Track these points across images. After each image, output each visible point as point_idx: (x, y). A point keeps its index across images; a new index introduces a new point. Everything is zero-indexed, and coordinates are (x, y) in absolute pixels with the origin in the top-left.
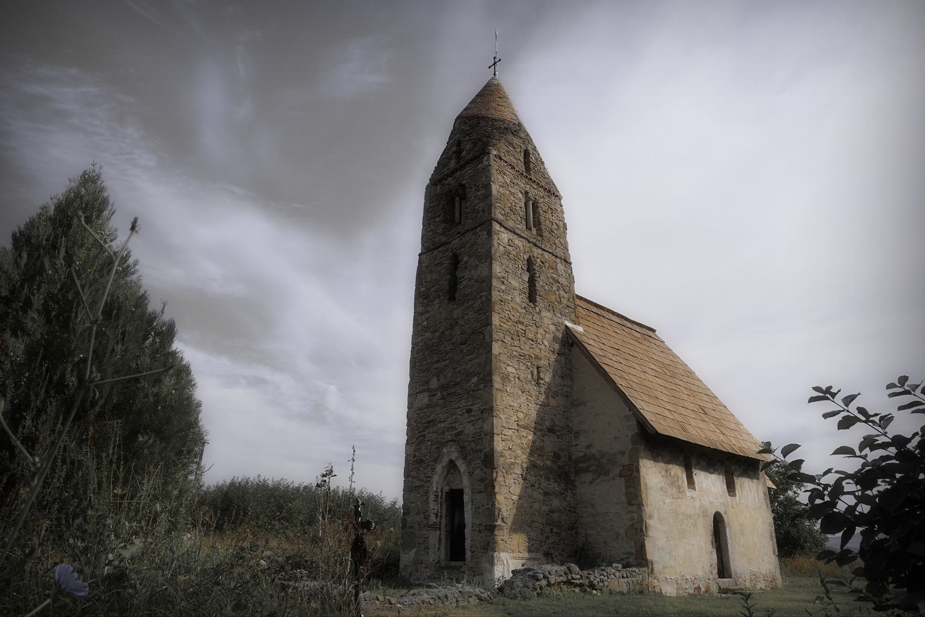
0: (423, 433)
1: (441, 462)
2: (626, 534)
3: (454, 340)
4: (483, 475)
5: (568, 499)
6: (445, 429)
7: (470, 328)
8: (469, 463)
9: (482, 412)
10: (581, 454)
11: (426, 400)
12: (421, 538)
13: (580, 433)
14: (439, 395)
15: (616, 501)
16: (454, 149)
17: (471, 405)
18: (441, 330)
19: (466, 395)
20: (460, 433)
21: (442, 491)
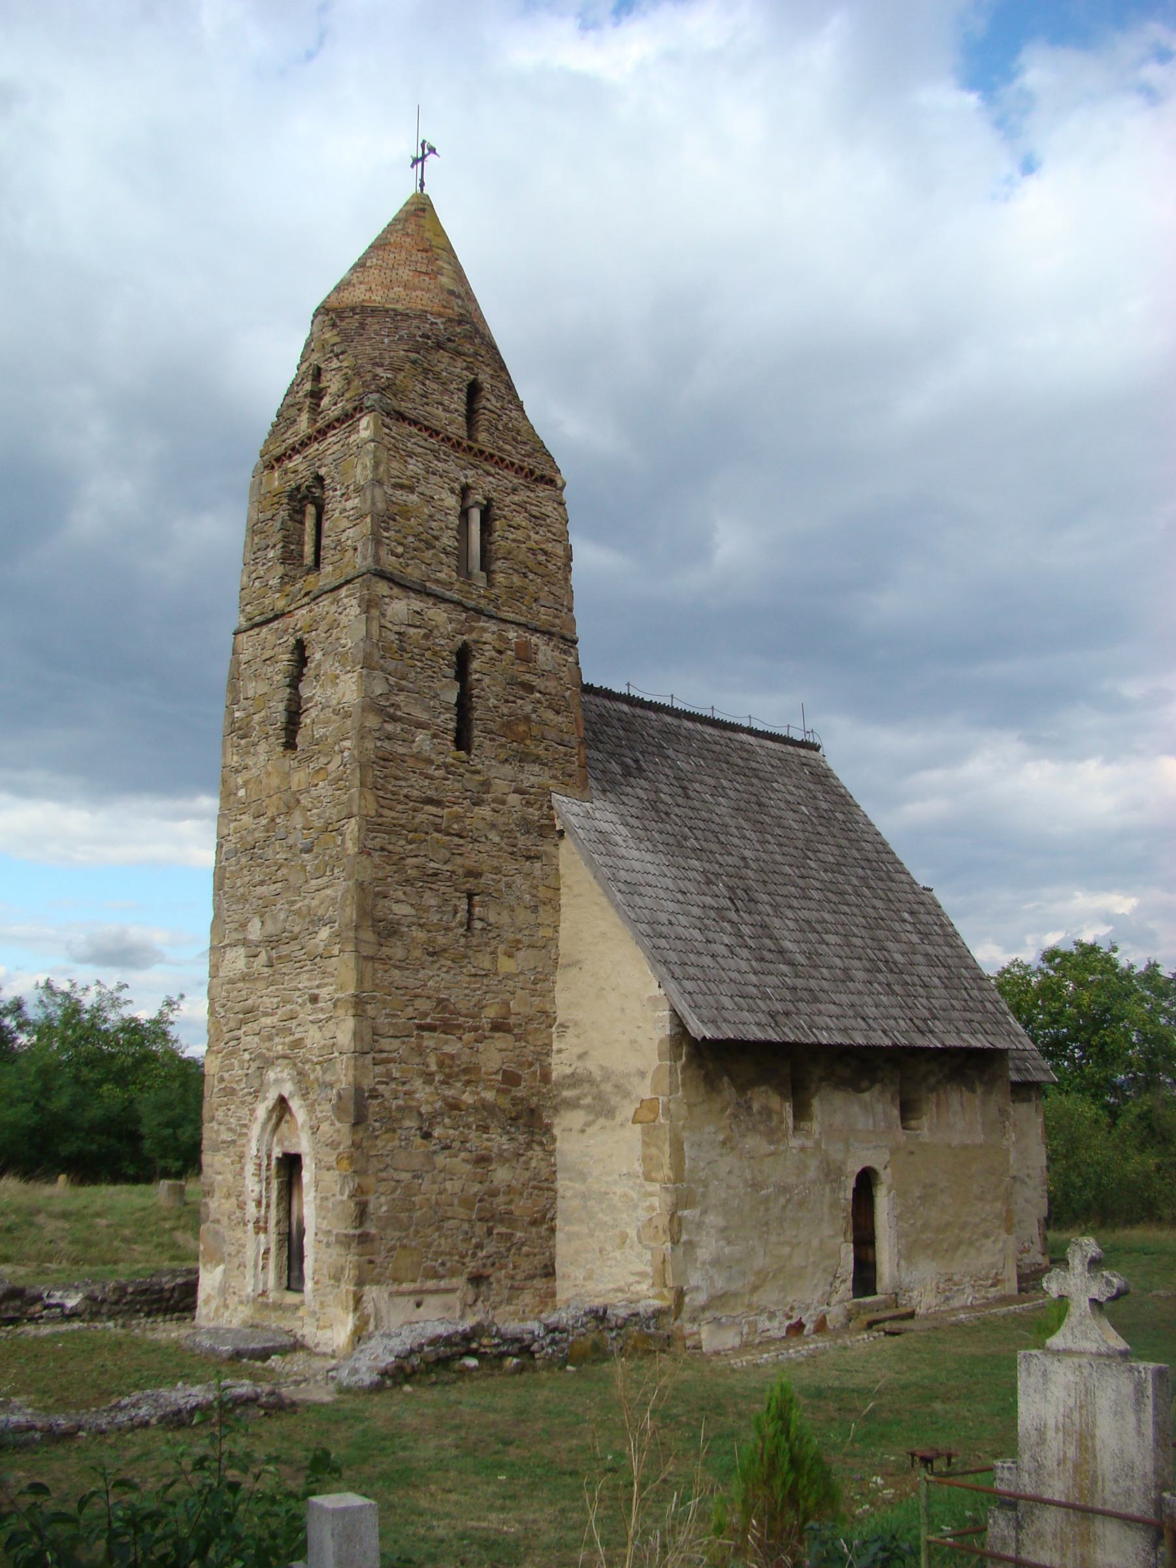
1: (265, 1099)
2: (639, 1237)
3: (290, 841)
4: (335, 1137)
5: (533, 1164)
6: (274, 1031)
8: (311, 1108)
9: (335, 1006)
10: (569, 1071)
11: (241, 964)
13: (567, 1027)
14: (263, 957)
15: (625, 1171)
16: (308, 386)
17: (318, 987)
18: (269, 814)
19: (309, 963)
21: (269, 1157)
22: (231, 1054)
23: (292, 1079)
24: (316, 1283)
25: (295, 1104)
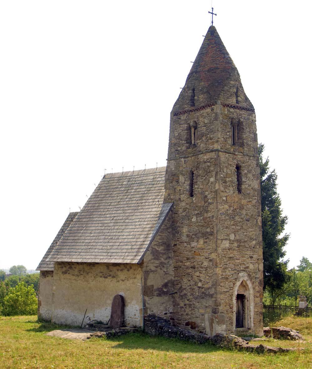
0: (226, 263)
1: (239, 281)
7: (250, 213)
8: (253, 283)
12: (228, 318)
17: (252, 255)
20: (248, 267)
22: (226, 268)
23: (247, 276)
24: (254, 324)
25: (249, 282)
